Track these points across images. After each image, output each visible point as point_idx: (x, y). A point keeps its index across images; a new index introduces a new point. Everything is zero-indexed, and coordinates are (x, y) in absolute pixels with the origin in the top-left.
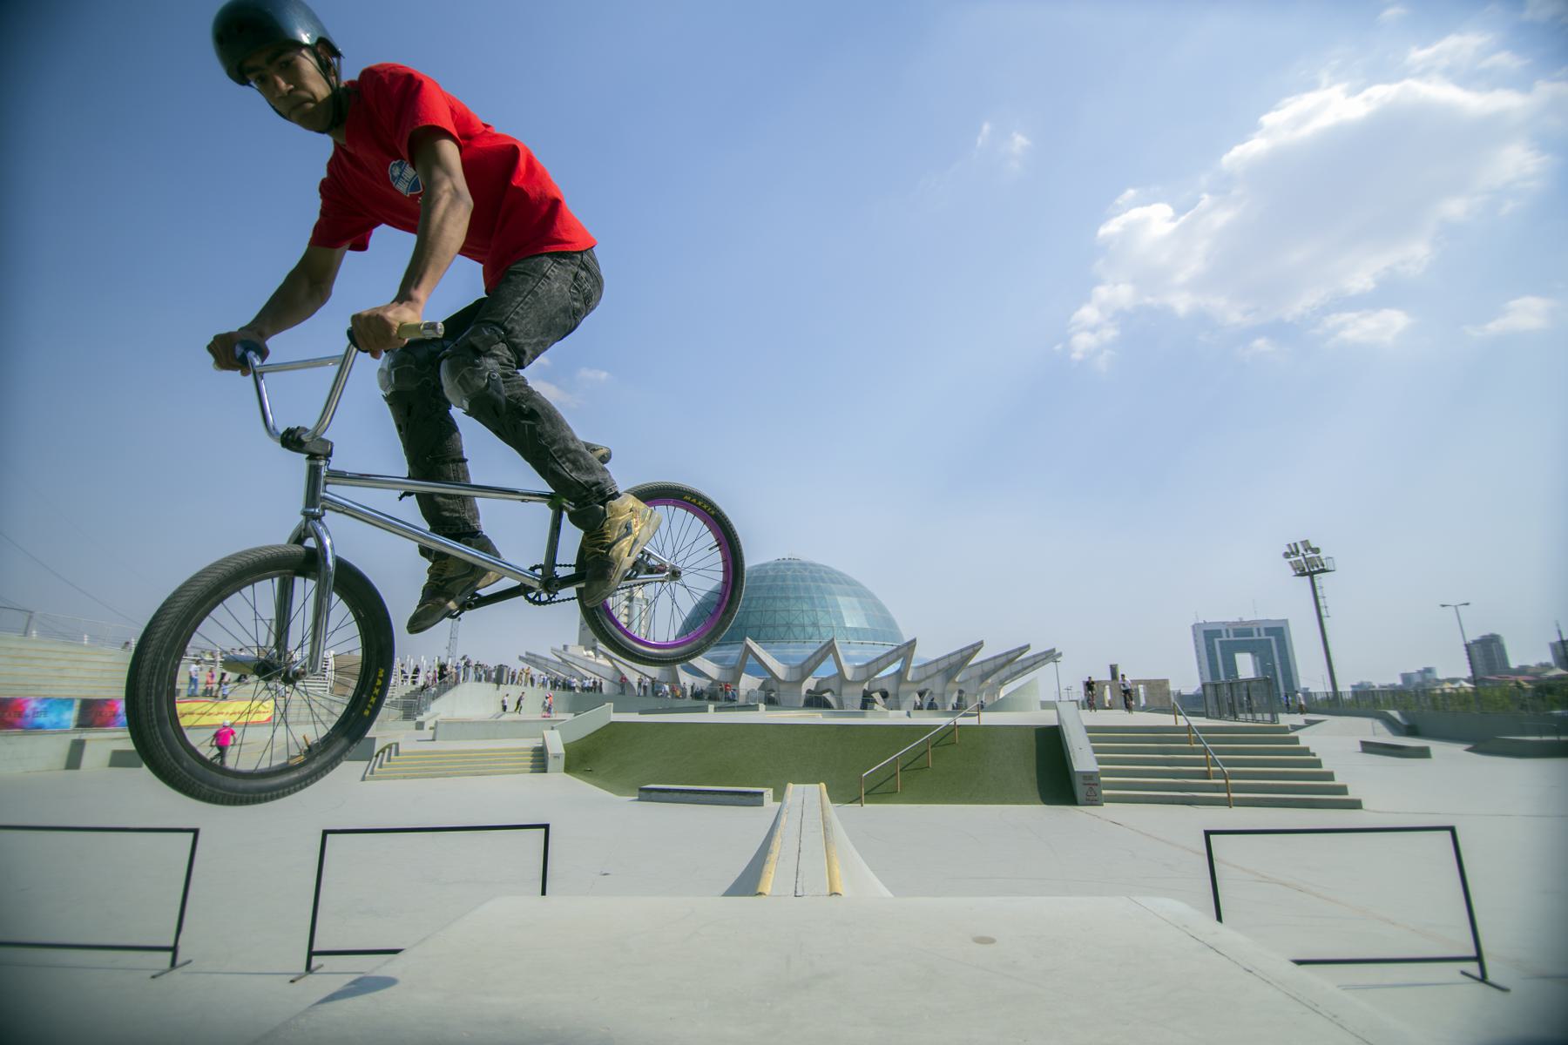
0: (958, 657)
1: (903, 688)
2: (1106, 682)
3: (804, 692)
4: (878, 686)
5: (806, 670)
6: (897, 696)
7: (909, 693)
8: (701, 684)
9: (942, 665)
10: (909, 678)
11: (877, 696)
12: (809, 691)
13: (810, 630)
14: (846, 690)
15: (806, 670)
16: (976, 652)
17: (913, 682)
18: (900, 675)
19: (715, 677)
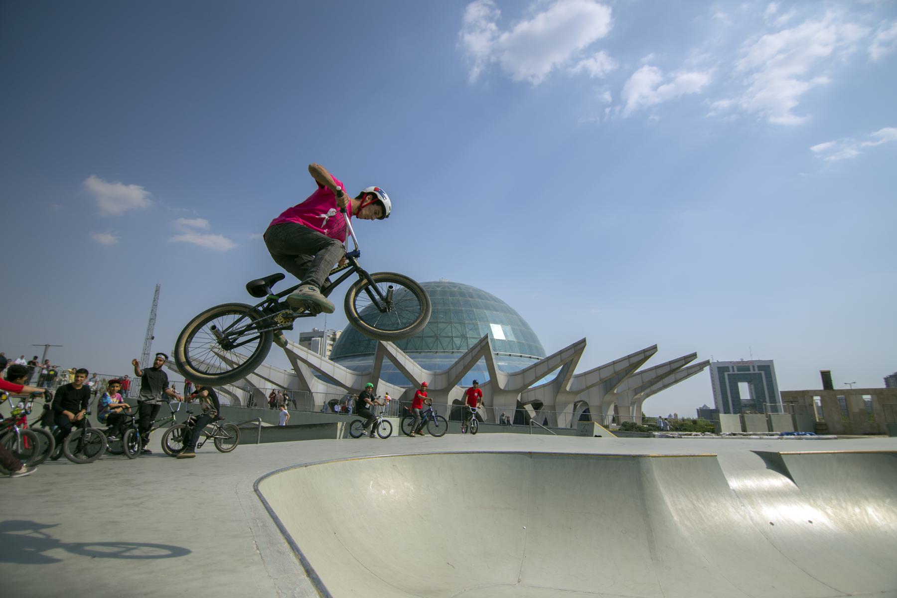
0: (626, 364)
1: (561, 398)
2: (816, 393)
3: (450, 403)
4: (532, 398)
5: (452, 378)
6: (553, 407)
7: (565, 404)
8: (338, 393)
9: (605, 374)
10: (568, 388)
11: (529, 408)
12: (456, 402)
13: (457, 341)
14: (499, 400)
15: (452, 378)
16: (646, 358)
17: (571, 392)
18: (557, 384)
19: (349, 384)
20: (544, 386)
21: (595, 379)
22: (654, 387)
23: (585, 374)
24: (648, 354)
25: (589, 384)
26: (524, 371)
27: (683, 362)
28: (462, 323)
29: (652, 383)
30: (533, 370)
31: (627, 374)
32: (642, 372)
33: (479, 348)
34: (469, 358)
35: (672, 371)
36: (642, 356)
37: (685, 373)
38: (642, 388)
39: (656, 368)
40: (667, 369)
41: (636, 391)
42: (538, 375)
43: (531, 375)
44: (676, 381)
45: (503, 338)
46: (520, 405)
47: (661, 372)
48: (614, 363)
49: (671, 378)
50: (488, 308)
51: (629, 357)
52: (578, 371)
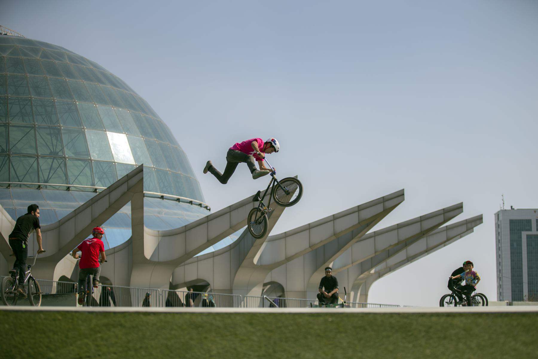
0: (353, 220)
9: (320, 237)
16: (387, 211)
18: (239, 253)
20: (213, 255)
21: (300, 245)
22: (392, 261)
23: (286, 236)
24: (389, 204)
25: (291, 252)
26: (188, 229)
27: (441, 218)
28: (57, 133)
29: (390, 253)
30: (203, 227)
31: (353, 239)
32: (376, 234)
33: (124, 188)
34: (104, 204)
35: (423, 233)
36: (379, 209)
37: (443, 237)
38: (373, 262)
39: (399, 226)
40: (415, 230)
41: (364, 267)
42: (213, 235)
43: (199, 236)
44: (428, 250)
45: (134, 163)
46: (173, 286)
47: (406, 234)
48: (335, 218)
49: (421, 244)
50: (103, 101)
51: (360, 209)
52: (277, 230)
